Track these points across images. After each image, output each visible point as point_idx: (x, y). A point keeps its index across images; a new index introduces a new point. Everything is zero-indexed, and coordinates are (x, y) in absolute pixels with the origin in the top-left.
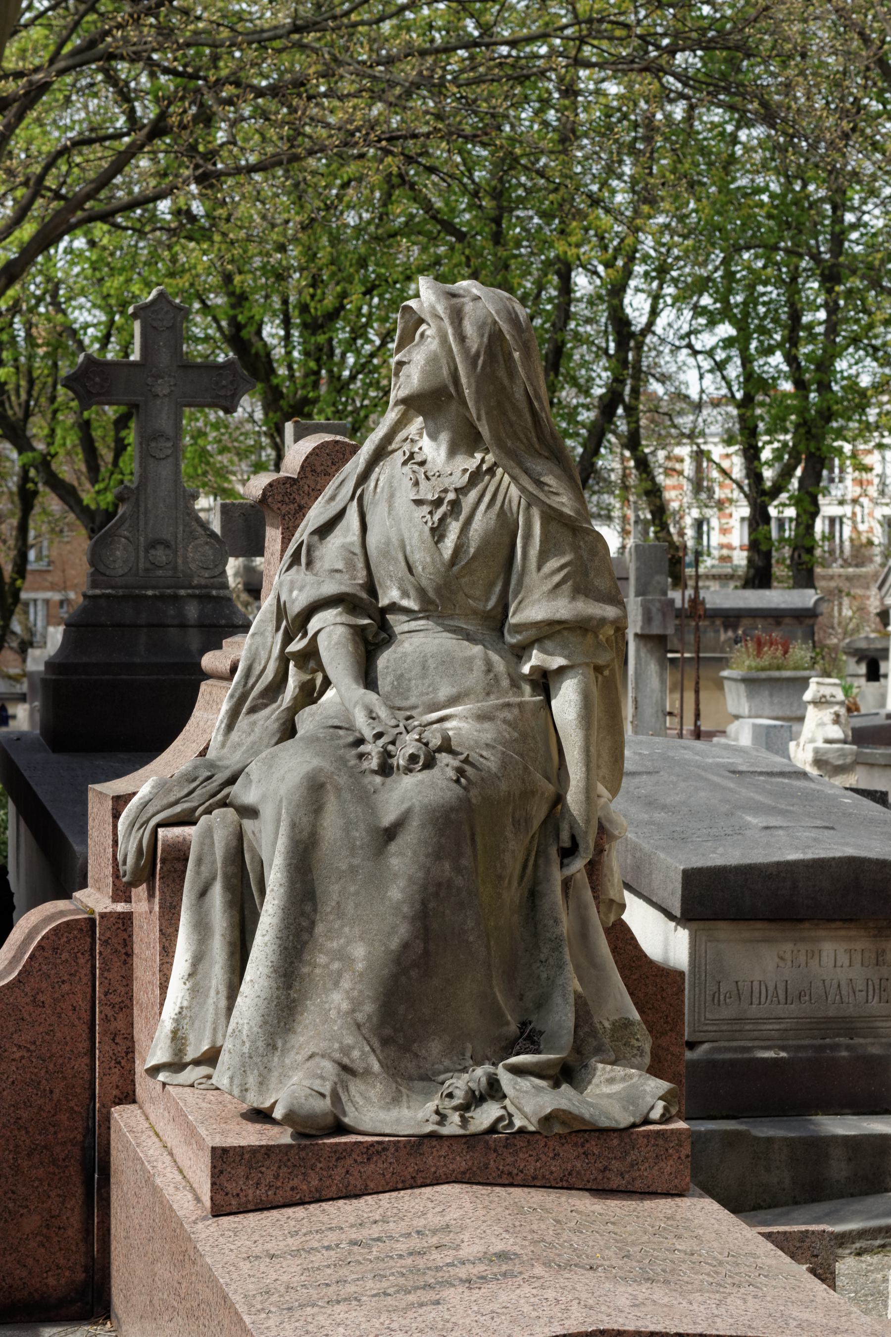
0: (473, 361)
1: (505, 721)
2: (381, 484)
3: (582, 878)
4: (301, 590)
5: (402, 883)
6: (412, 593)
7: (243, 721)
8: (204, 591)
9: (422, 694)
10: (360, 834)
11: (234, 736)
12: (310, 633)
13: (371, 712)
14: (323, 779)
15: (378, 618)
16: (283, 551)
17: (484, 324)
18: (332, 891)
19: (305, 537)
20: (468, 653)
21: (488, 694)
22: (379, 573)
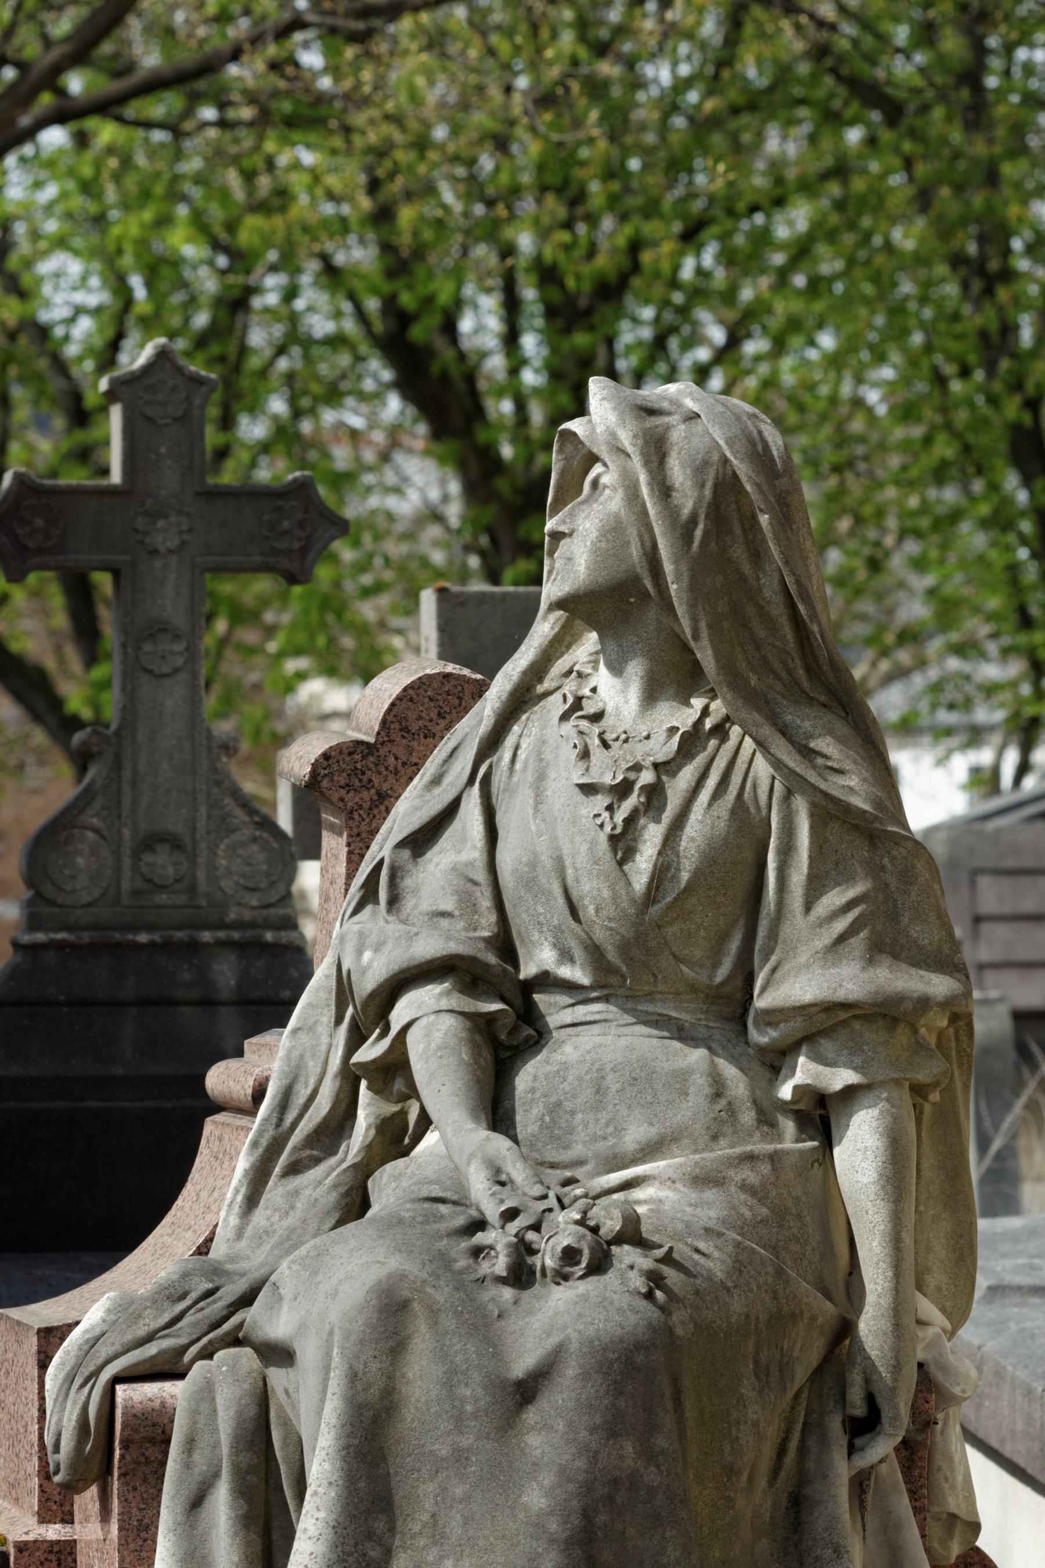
0: (684, 532)
1: (744, 1187)
2: (522, 755)
3: (892, 1473)
5: (547, 1479)
6: (578, 953)
7: (275, 1191)
8: (249, 934)
9: (595, 1139)
10: (472, 1392)
11: (260, 1217)
12: (395, 1029)
13: (498, 1171)
14: (406, 1293)
15: (518, 1001)
16: (350, 876)
17: (706, 463)
18: (423, 1495)
20: (681, 1063)
21: (715, 1138)
22: (519, 919)
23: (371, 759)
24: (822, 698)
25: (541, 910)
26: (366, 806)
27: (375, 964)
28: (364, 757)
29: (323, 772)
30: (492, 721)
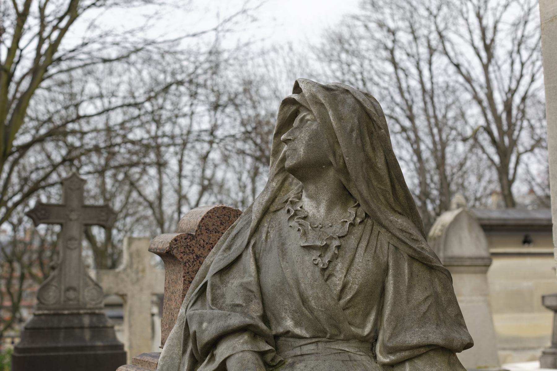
4: (210, 322)
12: (219, 360)
16: (185, 290)
19: (208, 278)
23: (194, 241)
24: (400, 211)
25: (286, 303)
27: (209, 329)
28: (191, 241)
29: (174, 246)
30: (256, 221)
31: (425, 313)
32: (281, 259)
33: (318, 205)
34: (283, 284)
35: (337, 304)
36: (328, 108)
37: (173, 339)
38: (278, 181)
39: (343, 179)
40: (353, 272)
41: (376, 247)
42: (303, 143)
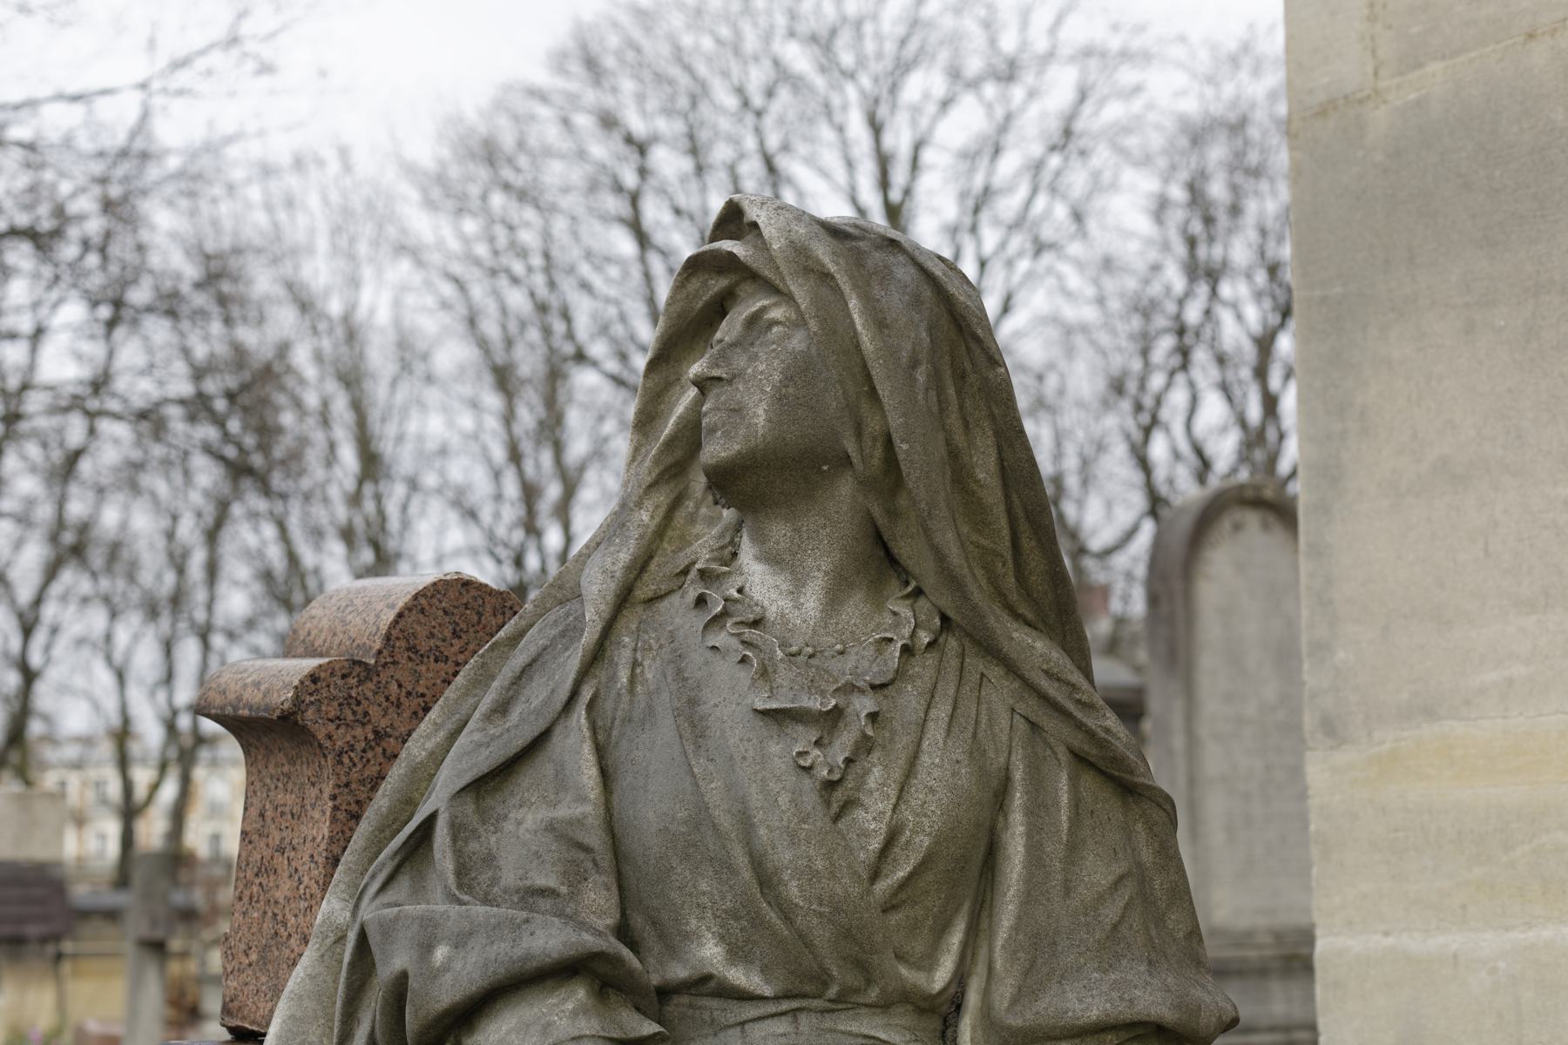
4: (460, 942)
16: (340, 840)
19: (437, 799)
23: (370, 685)
24: (1030, 616)
25: (704, 886)
26: (360, 746)
27: (458, 965)
28: (360, 682)
29: (308, 699)
30: (599, 628)
31: (1115, 927)
32: (690, 749)
33: (797, 587)
34: (697, 827)
35: (869, 892)
36: (846, 288)
37: (300, 997)
38: (657, 507)
39: (877, 511)
40: (916, 796)
41: (977, 722)
42: (763, 392)
